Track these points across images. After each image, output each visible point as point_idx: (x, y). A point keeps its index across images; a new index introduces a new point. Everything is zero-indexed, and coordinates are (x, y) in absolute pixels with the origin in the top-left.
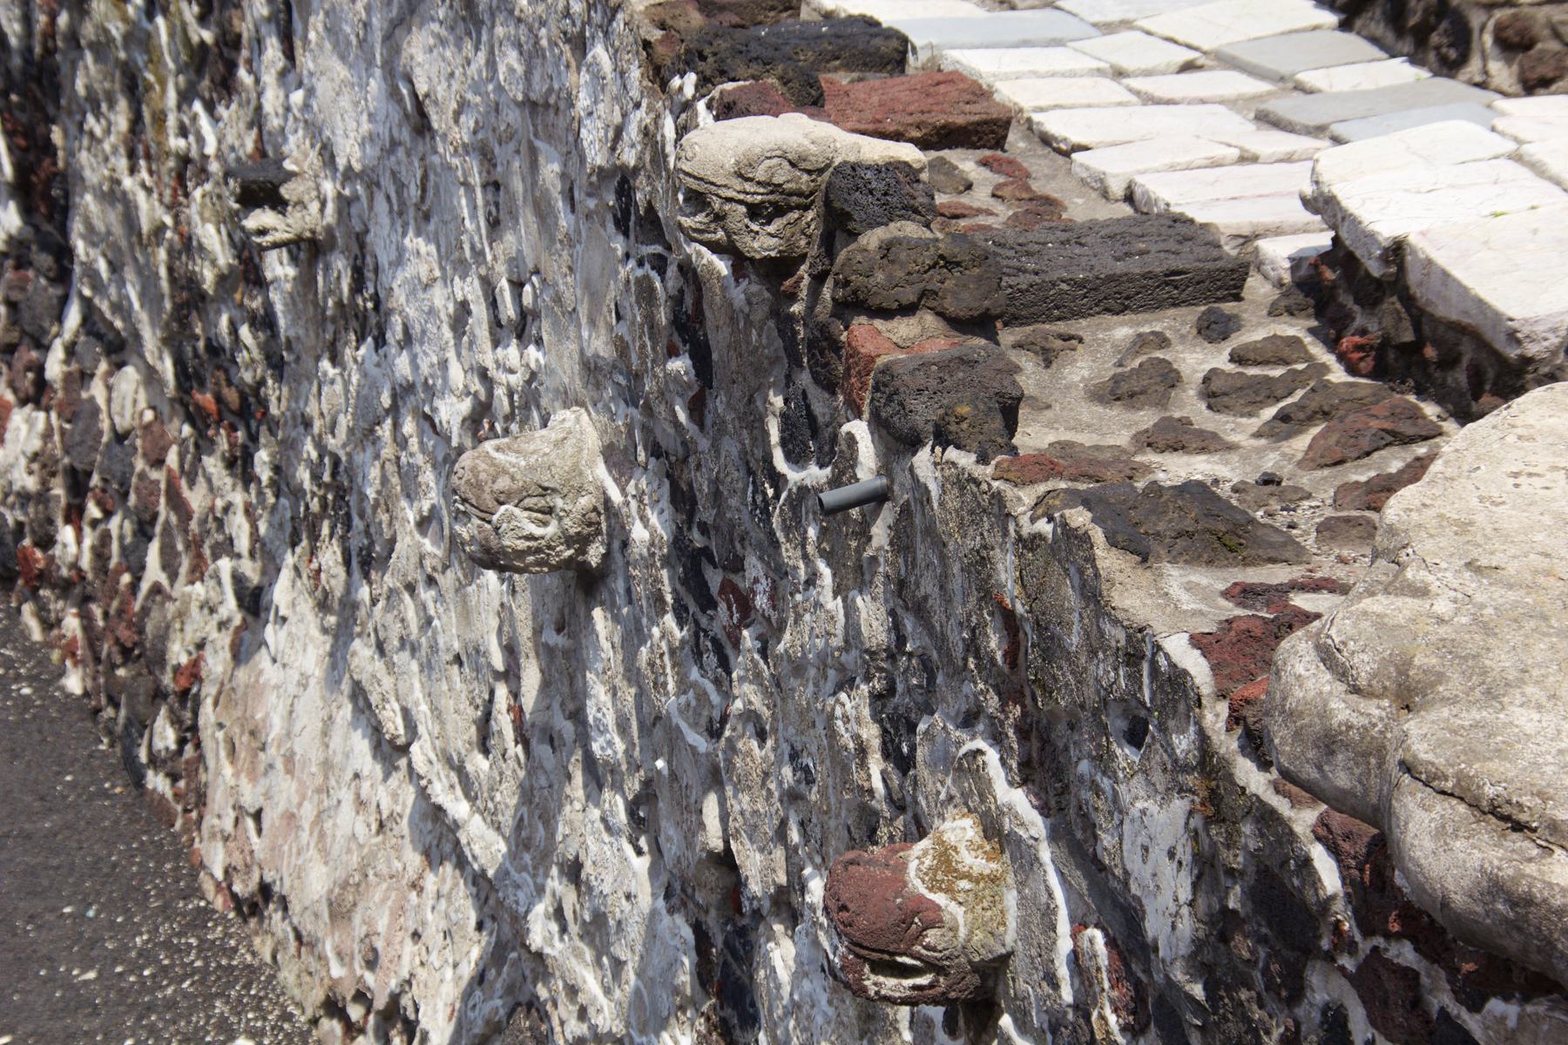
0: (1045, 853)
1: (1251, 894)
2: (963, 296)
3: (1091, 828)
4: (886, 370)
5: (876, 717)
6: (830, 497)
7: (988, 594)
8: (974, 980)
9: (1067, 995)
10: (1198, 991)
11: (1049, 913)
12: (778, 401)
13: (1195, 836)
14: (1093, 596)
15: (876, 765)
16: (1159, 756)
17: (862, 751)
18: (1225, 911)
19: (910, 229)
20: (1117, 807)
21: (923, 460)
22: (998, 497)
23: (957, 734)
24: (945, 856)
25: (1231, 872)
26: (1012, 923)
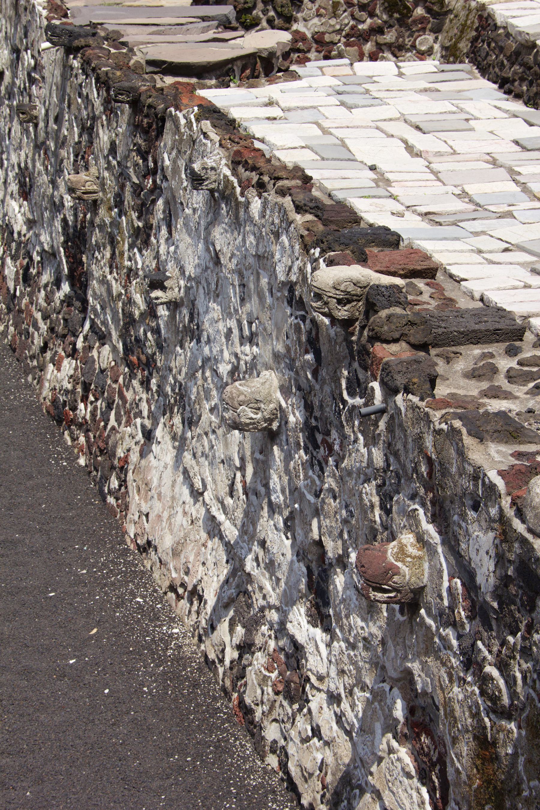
0: (440, 549)
1: (516, 570)
2: (417, 337)
3: (457, 541)
4: (387, 363)
5: (378, 494)
6: (364, 410)
7: (422, 450)
8: (412, 595)
9: (446, 603)
10: (495, 605)
11: (440, 572)
12: (346, 373)
13: (497, 547)
14: (461, 453)
15: (377, 512)
16: (484, 516)
17: (372, 506)
18: (507, 575)
19: (398, 310)
20: (468, 534)
21: (399, 398)
22: (427, 414)
23: (408, 502)
24: (402, 548)
25: (509, 561)
26: (426, 575)
